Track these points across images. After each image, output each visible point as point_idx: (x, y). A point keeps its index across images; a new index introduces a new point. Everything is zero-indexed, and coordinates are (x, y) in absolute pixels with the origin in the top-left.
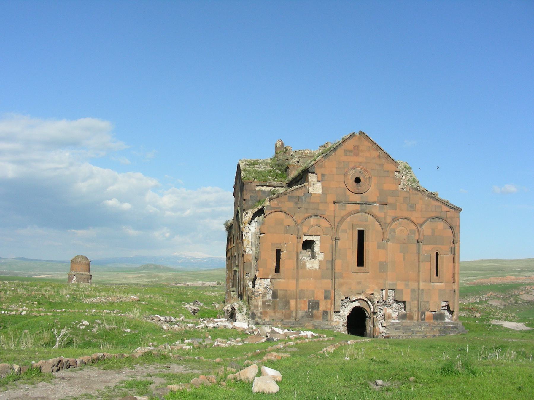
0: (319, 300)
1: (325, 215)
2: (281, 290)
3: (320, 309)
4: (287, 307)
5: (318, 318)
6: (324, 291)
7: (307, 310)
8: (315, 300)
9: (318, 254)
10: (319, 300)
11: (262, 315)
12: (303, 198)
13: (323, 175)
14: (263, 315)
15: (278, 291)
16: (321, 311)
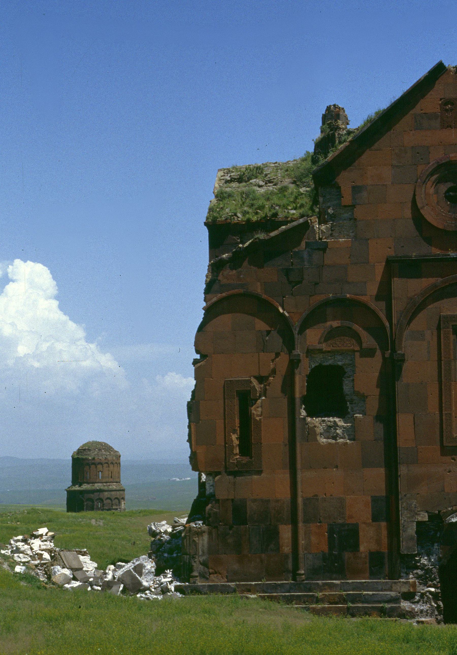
0: (356, 525)
1: (366, 295)
2: (254, 501)
3: (362, 548)
4: (272, 546)
5: (356, 573)
6: (369, 499)
7: (327, 551)
8: (348, 525)
9: (352, 402)
10: (356, 525)
11: (208, 568)
12: (305, 255)
13: (356, 190)
14: (212, 569)
15: (248, 503)
16: (363, 555)
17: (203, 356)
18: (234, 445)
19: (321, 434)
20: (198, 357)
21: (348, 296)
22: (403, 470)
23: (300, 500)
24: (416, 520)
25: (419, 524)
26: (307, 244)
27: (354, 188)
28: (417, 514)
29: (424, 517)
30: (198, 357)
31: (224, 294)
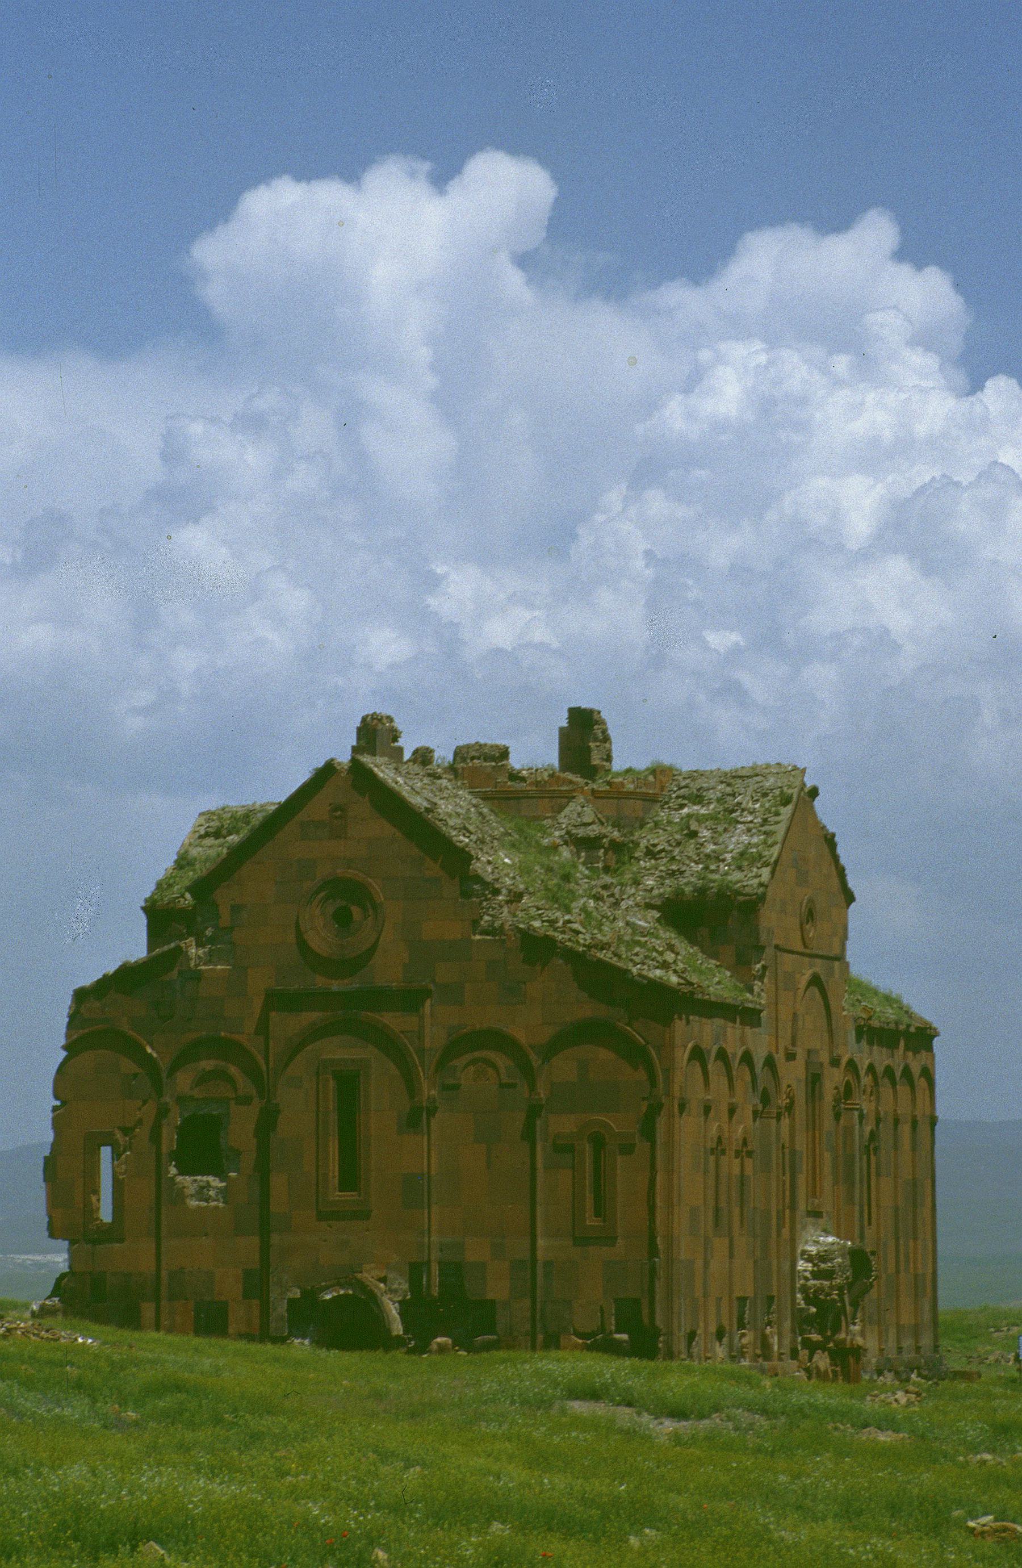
13: (236, 909)
17: (64, 1103)
18: (94, 1208)
19: (192, 1196)
20: (58, 1103)
21: (223, 1034)
22: (275, 1239)
23: (164, 1273)
24: (287, 1297)
25: (291, 1301)
26: (180, 973)
27: (232, 907)
28: (288, 1290)
29: (296, 1293)
30: (58, 1103)
31: (86, 1031)
